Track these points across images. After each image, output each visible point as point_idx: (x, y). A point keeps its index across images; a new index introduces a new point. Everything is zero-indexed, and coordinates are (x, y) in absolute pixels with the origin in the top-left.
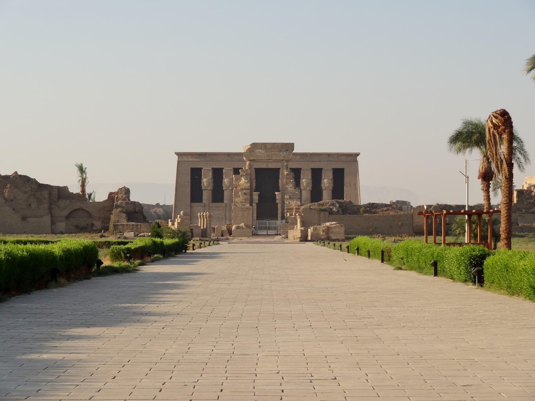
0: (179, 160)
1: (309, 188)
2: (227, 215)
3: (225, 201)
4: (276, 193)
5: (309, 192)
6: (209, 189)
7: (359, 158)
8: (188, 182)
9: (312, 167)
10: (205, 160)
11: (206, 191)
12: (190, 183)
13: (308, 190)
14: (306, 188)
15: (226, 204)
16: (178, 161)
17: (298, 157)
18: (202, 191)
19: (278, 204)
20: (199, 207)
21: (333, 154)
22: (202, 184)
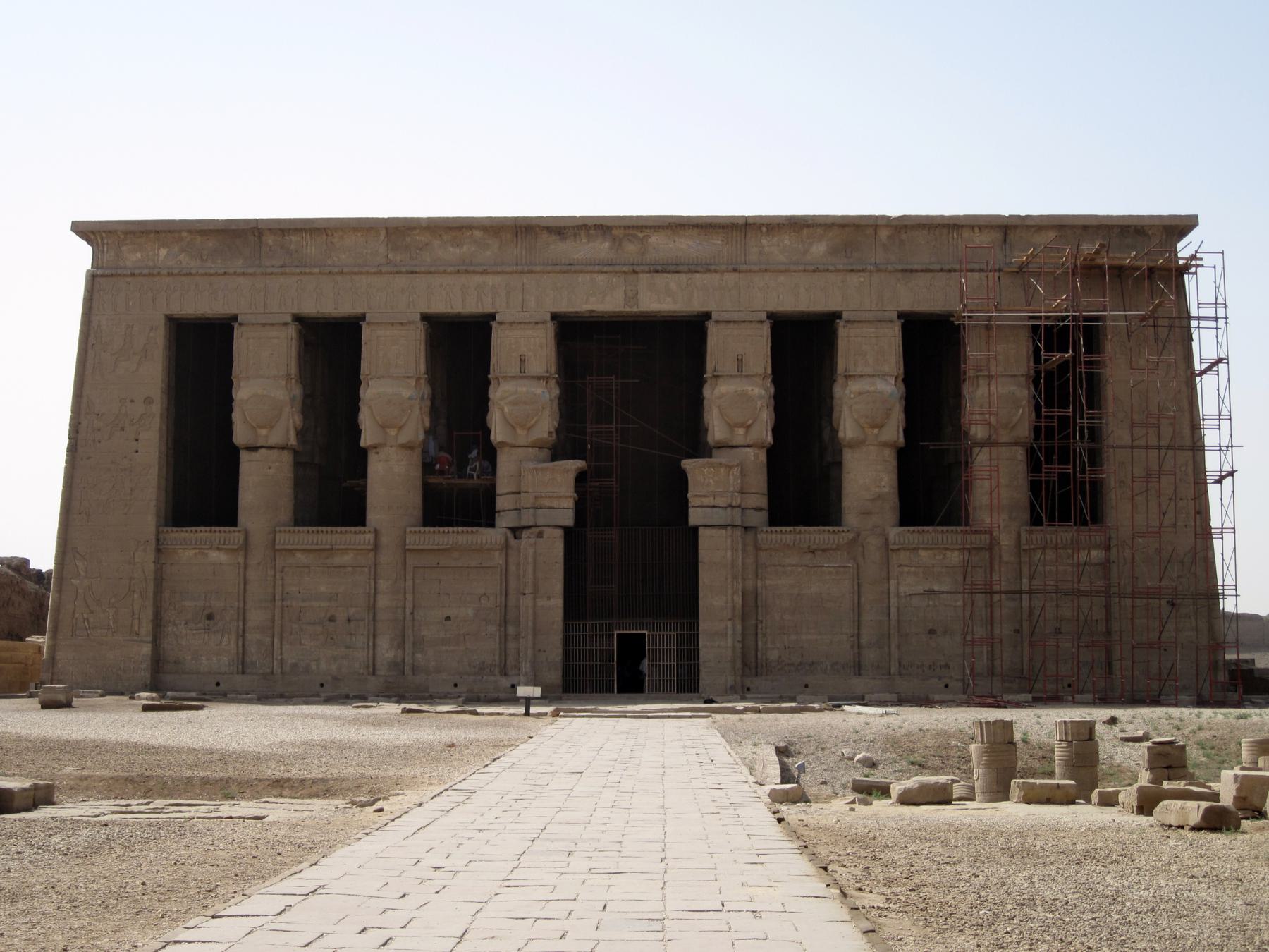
0: (100, 272)
1: (894, 431)
2: (383, 601)
3: (372, 516)
4: (687, 464)
5: (890, 456)
6: (276, 438)
7: (1185, 248)
8: (148, 401)
9: (906, 306)
10: (250, 271)
11: (256, 455)
12: (157, 408)
13: (885, 445)
14: (869, 431)
15: (376, 532)
16: (93, 280)
17: (819, 249)
18: (230, 456)
19: (701, 531)
20: (214, 555)
21: (1028, 227)
22: (233, 415)
